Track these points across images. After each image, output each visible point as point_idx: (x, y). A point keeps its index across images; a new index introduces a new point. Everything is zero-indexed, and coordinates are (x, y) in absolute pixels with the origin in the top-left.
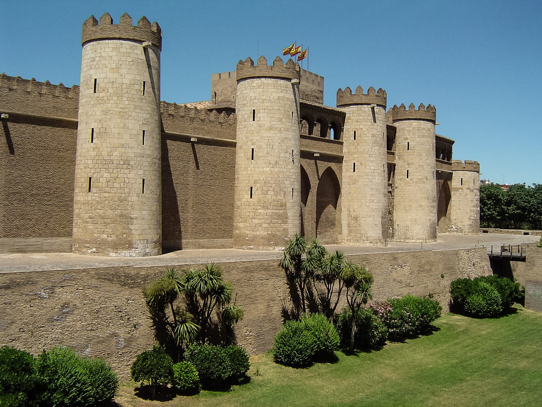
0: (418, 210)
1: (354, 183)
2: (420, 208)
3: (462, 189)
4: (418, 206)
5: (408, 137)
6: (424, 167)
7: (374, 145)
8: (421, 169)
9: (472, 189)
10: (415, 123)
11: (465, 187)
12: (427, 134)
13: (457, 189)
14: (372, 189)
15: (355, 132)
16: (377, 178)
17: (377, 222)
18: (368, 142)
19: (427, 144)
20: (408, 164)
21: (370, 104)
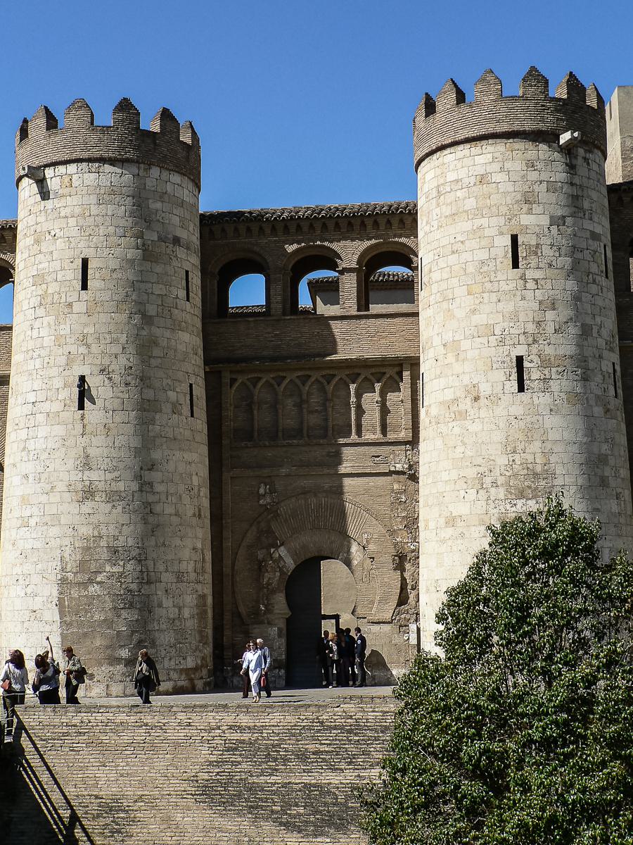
0: (443, 541)
2: (450, 531)
4: (442, 521)
6: (466, 345)
8: (451, 358)
12: (471, 203)
14: (26, 477)
16: (42, 432)
17: (37, 603)
19: (473, 244)
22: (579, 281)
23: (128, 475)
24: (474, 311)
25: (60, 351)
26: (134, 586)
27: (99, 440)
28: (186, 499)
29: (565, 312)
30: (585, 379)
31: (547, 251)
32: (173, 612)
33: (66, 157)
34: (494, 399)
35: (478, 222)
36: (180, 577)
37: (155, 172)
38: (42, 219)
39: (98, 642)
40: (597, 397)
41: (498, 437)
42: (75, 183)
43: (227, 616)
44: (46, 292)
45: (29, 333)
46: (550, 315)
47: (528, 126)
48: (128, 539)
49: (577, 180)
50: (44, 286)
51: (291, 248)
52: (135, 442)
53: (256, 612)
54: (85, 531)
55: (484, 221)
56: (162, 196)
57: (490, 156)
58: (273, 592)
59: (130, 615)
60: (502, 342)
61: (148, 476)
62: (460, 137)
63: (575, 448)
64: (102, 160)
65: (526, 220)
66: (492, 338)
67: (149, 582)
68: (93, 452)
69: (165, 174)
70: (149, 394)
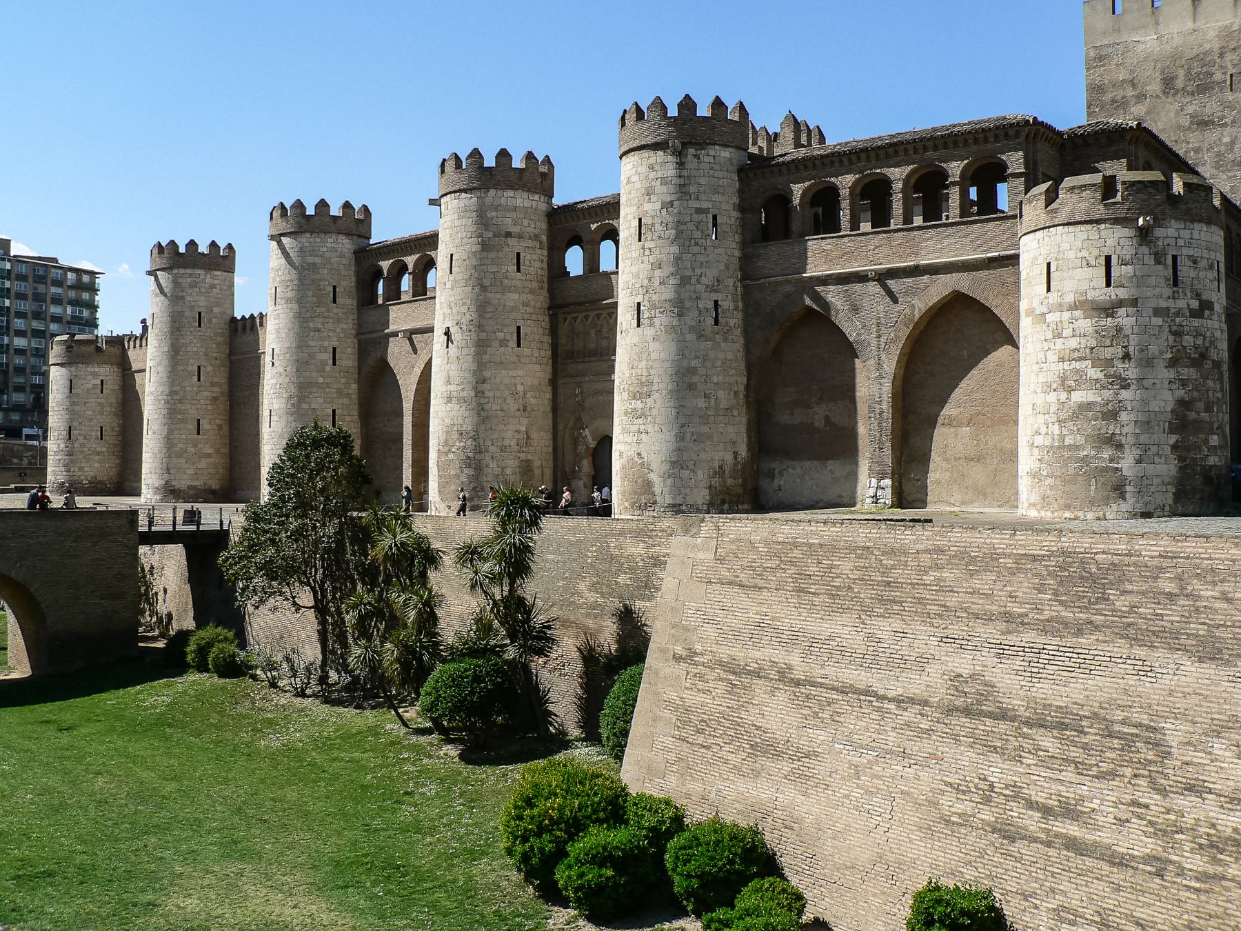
22: (682, 246)
23: (470, 387)
26: (471, 455)
27: (454, 366)
28: (510, 400)
29: (668, 269)
30: (680, 315)
31: (658, 227)
32: (498, 471)
36: (503, 449)
37: (492, 192)
39: (453, 488)
40: (691, 329)
43: (559, 474)
46: (658, 272)
47: (649, 141)
48: (468, 426)
49: (685, 173)
51: (593, 227)
52: (474, 367)
53: (574, 471)
54: (448, 421)
56: (497, 208)
58: (582, 458)
59: (470, 472)
61: (481, 387)
63: (668, 364)
64: (460, 191)
65: (647, 207)
67: (480, 452)
68: (452, 374)
69: (499, 193)
70: (483, 336)
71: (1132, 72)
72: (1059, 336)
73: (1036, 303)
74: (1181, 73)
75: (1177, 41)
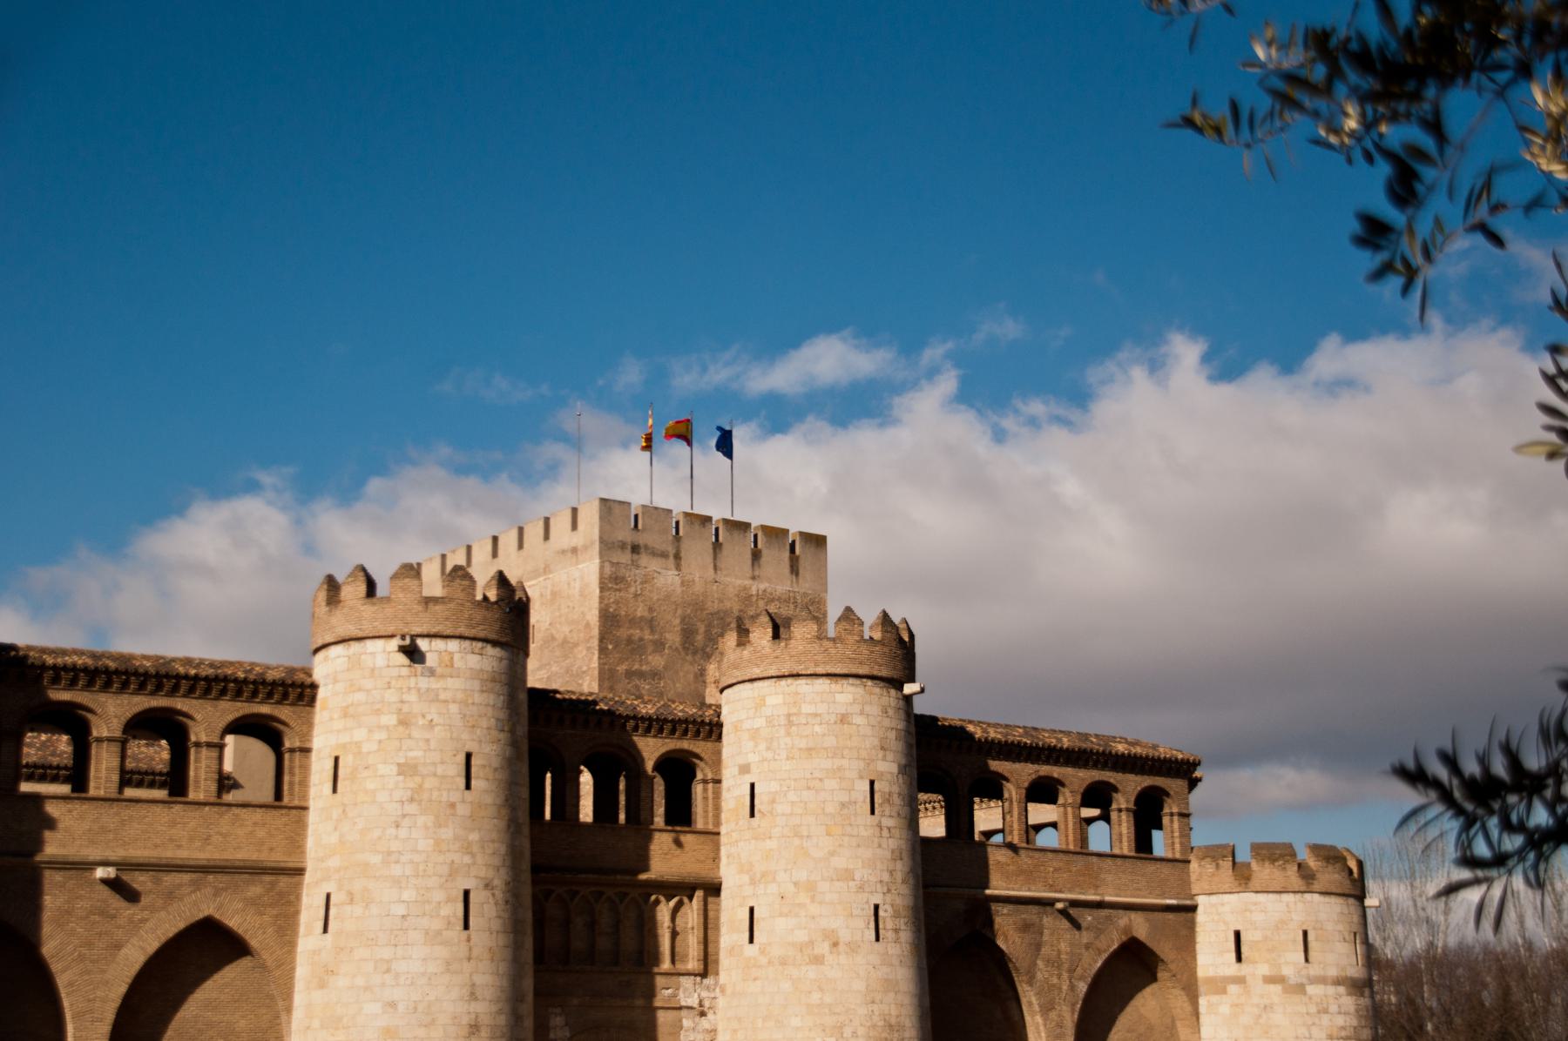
1: (322, 985)
3: (1240, 980)
5: (752, 758)
6: (824, 886)
7: (411, 808)
8: (803, 898)
9: (1293, 980)
10: (775, 695)
11: (1257, 968)
12: (831, 741)
13: (1220, 985)
14: (393, 1005)
15: (337, 759)
18: (382, 797)
19: (832, 784)
20: (753, 882)
21: (392, 636)
24: (832, 854)
25: (441, 859)
33: (448, 632)
34: (853, 948)
35: (838, 762)
38: (413, 697)
41: (859, 985)
42: (458, 663)
44: (421, 786)
45: (392, 831)
50: (418, 779)
55: (845, 763)
57: (850, 697)
60: (861, 888)
62: (820, 670)
66: (851, 884)
71: (651, 610)
72: (1326, 1011)
73: (1287, 971)
74: (702, 628)
75: (698, 588)
